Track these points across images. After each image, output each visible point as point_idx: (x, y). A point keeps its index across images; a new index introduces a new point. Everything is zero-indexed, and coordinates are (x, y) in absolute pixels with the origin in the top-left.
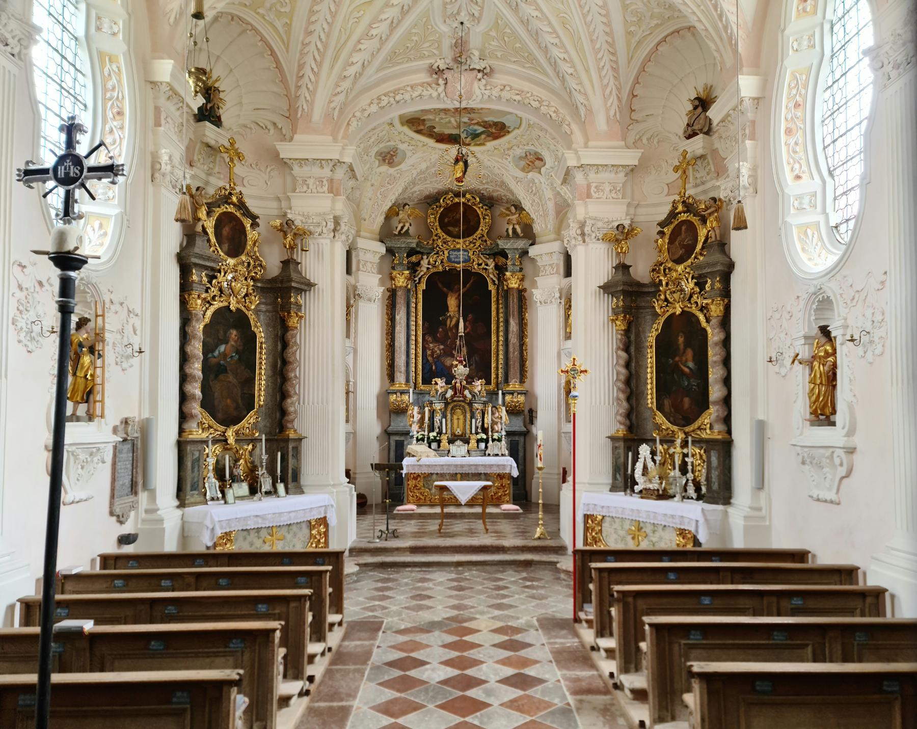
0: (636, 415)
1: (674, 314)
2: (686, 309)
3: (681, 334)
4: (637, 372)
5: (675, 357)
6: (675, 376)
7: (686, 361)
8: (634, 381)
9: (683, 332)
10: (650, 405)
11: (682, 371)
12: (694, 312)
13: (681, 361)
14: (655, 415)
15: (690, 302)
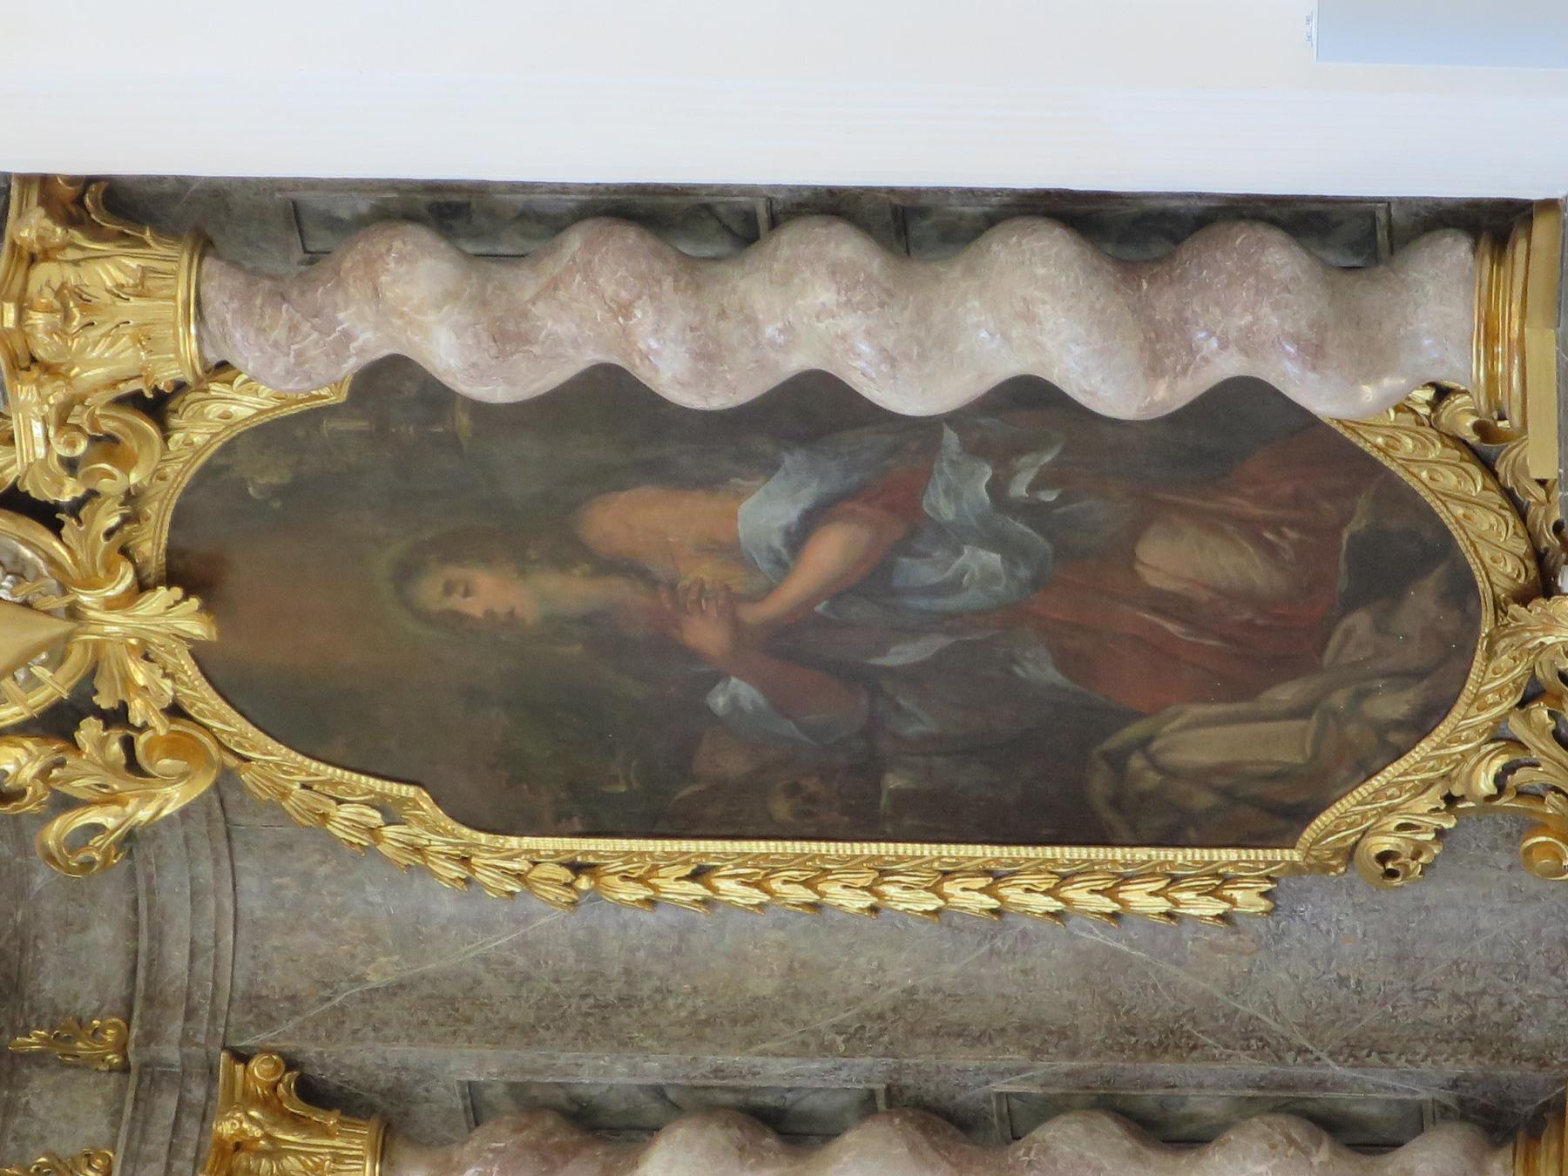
0: (1352, 1051)
1: (200, 654)
2: (151, 544)
3: (430, 591)
4: (856, 1036)
5: (692, 655)
6: (901, 655)
7: (729, 550)
8: (964, 1059)
9: (406, 573)
10: (1247, 899)
11: (841, 591)
12: (180, 473)
13: (734, 600)
14: (1350, 854)
15: (75, 508)
